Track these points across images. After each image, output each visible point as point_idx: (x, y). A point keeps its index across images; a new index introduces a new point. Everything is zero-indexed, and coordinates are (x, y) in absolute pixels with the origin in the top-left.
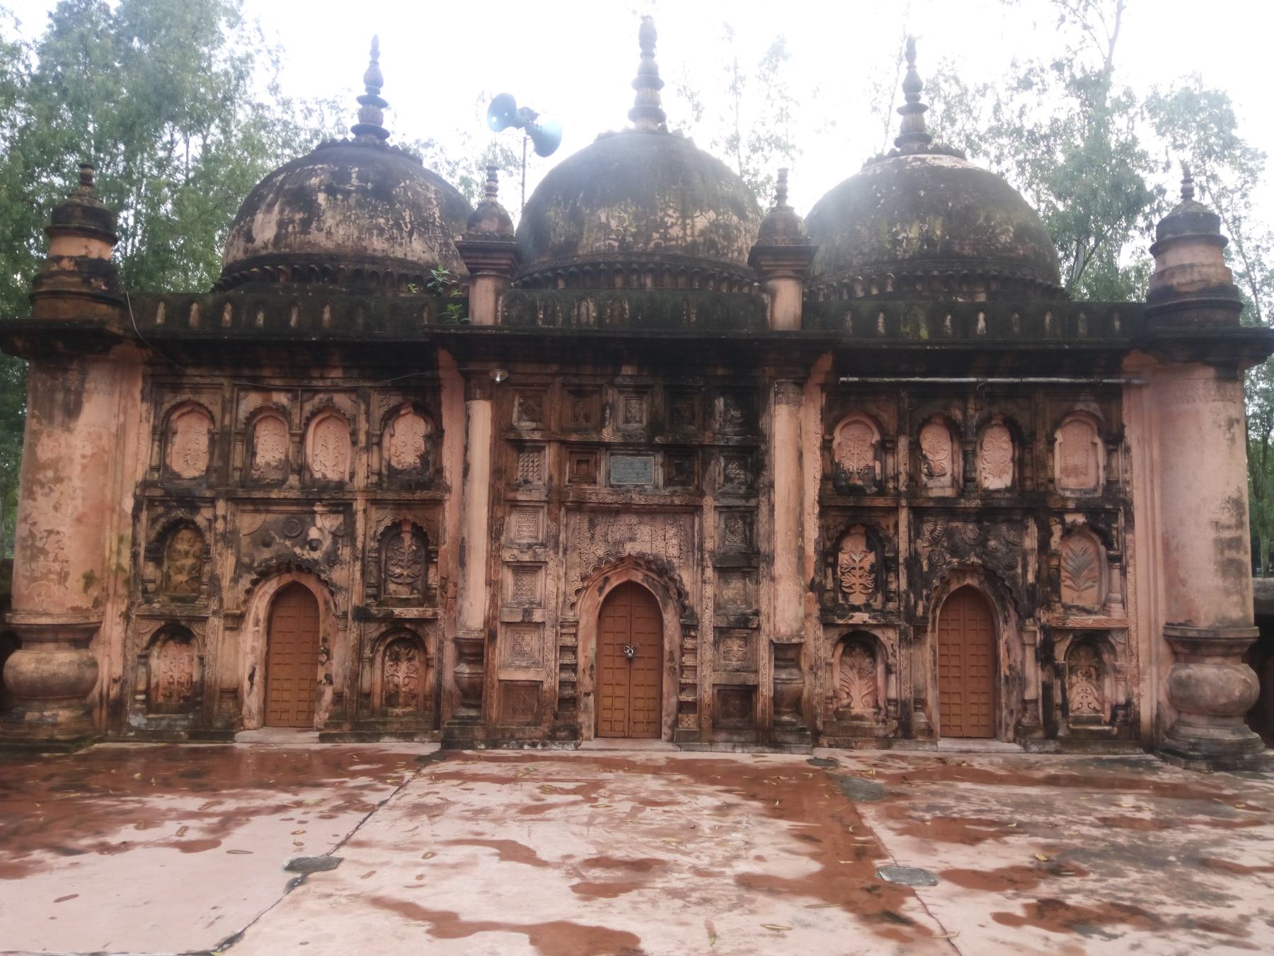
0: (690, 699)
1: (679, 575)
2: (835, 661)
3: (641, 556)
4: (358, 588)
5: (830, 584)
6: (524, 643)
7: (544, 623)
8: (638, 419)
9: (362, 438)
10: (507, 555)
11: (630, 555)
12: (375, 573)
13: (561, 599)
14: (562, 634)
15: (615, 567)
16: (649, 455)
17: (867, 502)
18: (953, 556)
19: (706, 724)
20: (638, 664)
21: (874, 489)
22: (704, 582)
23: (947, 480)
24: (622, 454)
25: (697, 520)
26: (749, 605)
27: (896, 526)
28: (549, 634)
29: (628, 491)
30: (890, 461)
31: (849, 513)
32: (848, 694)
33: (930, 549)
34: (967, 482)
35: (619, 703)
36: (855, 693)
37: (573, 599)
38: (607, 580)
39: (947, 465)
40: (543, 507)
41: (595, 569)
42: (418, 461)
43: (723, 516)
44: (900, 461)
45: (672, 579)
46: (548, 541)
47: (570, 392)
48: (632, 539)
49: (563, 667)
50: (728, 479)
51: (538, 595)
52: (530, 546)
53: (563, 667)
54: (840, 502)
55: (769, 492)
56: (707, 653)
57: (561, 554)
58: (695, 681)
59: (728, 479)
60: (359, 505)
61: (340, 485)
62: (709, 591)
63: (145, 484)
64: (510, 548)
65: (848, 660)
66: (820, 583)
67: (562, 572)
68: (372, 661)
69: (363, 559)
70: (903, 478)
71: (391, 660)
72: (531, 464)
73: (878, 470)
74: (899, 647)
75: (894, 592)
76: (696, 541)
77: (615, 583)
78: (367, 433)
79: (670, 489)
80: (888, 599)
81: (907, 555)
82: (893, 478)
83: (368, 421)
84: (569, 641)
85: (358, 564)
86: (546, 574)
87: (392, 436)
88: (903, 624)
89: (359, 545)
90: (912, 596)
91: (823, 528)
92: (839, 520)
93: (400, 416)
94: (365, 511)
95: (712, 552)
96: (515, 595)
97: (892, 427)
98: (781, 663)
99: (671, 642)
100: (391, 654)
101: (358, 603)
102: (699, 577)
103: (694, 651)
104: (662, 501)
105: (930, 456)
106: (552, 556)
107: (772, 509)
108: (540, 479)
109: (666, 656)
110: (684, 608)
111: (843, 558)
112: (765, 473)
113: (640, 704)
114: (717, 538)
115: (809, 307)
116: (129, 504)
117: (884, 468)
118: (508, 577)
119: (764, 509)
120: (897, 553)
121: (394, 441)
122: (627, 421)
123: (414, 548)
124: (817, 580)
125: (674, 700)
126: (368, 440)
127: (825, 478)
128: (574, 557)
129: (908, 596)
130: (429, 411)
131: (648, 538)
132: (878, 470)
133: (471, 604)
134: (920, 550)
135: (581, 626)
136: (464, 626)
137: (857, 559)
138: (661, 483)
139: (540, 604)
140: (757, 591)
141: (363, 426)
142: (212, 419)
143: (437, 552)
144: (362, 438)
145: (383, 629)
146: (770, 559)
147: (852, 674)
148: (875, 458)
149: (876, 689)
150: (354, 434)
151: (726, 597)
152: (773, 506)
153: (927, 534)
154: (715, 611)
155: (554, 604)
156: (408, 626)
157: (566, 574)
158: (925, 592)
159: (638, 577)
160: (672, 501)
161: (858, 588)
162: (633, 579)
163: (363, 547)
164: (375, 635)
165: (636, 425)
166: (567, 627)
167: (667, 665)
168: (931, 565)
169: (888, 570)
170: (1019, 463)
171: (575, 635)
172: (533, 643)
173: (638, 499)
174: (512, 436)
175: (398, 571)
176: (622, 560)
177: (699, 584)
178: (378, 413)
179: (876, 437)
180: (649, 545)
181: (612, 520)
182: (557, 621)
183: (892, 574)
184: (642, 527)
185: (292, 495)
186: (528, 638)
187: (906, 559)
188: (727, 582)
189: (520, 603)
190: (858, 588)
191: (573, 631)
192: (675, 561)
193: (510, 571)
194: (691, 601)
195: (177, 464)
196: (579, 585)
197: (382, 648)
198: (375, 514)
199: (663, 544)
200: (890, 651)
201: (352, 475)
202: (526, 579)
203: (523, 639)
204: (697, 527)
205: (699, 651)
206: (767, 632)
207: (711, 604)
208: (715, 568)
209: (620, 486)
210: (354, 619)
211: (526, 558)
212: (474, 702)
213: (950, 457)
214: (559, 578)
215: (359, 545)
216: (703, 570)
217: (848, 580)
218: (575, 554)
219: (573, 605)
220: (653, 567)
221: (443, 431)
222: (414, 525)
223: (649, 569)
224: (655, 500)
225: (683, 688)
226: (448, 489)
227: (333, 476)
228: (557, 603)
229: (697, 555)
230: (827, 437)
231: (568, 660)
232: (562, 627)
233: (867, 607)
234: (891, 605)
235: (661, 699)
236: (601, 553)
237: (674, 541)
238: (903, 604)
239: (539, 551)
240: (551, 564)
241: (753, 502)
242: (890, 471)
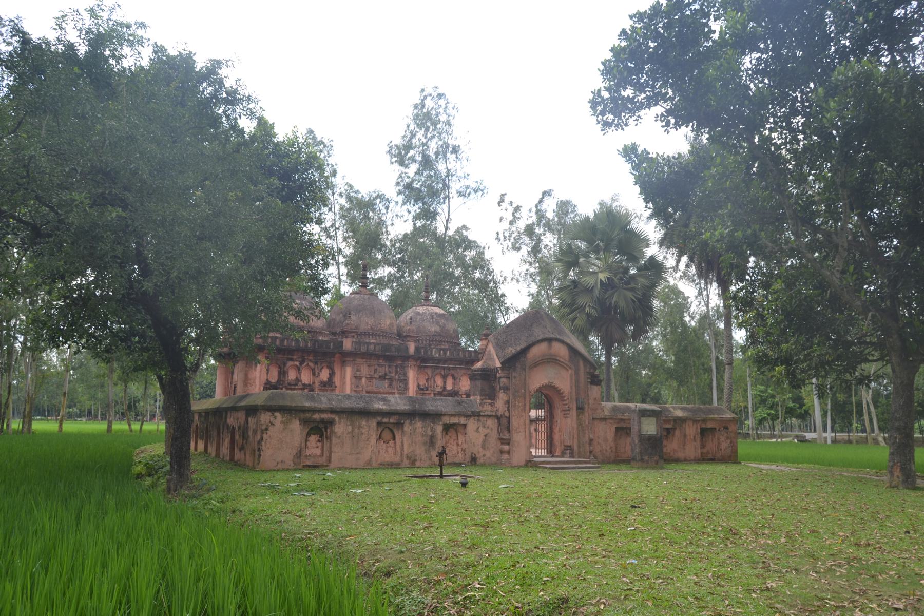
34: (444, 388)
44: (431, 383)
61: (309, 385)
63: (265, 384)
115: (417, 349)
116: (262, 388)
130: (331, 368)
142: (280, 367)
170: (454, 384)
173: (382, 390)
185: (301, 387)
195: (270, 380)
201: (314, 383)
226: (336, 387)
227: (307, 383)
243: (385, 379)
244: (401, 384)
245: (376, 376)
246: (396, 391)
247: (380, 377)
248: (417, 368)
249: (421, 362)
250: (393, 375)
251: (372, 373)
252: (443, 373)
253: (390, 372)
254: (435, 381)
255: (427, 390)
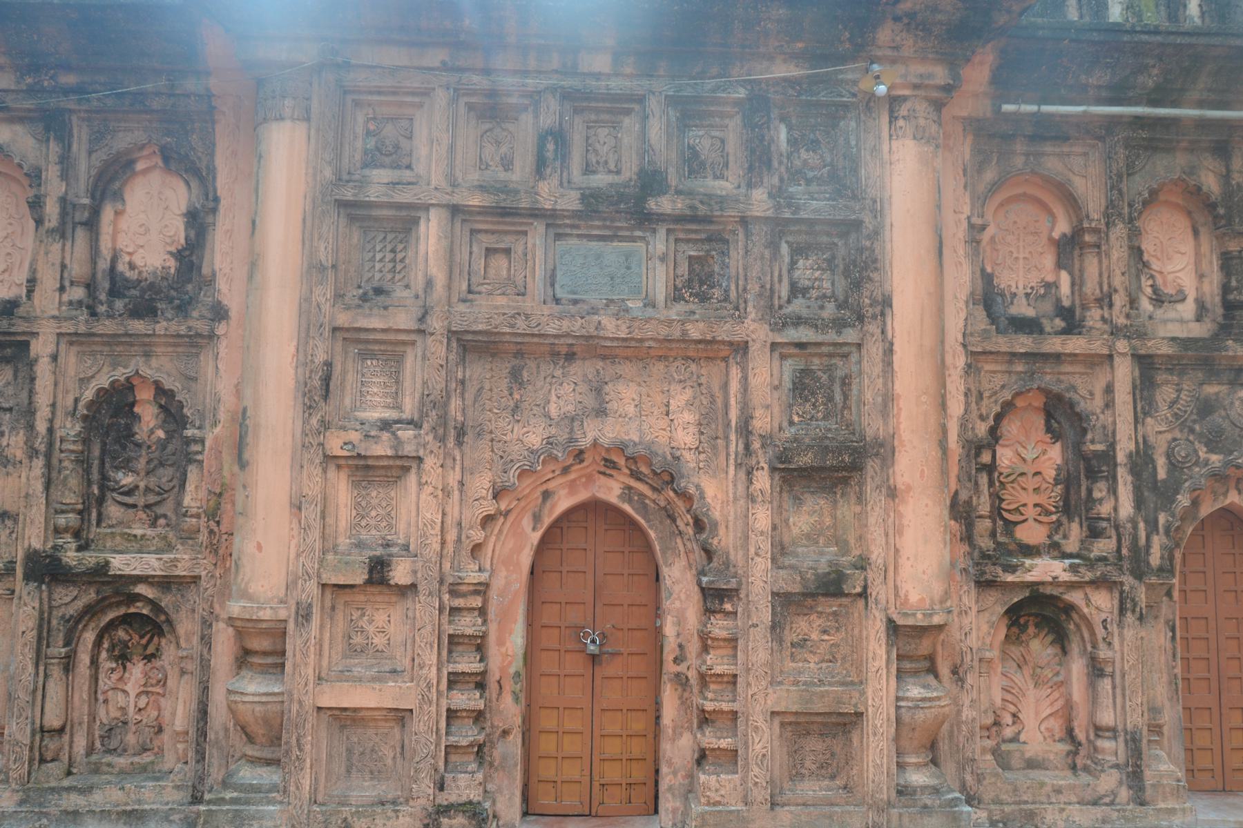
0: (724, 743)
1: (698, 487)
2: (994, 654)
3: (621, 448)
4: (37, 512)
5: (984, 505)
6: (371, 629)
7: (413, 586)
8: (612, 167)
9: (52, 210)
10: (335, 444)
11: (595, 444)
12: (74, 482)
13: (451, 536)
14: (454, 611)
15: (566, 470)
16: (633, 239)
17: (1054, 344)
18: (1211, 450)
19: (761, 794)
20: (611, 668)
21: (1059, 323)
22: (751, 498)
23: (1187, 309)
24: (579, 236)
25: (735, 373)
26: (844, 548)
27: (1109, 389)
28: (424, 609)
29: (594, 311)
30: (1092, 267)
31: (1020, 367)
32: (1014, 715)
33: (1169, 436)
35: (572, 745)
36: (1027, 716)
37: (478, 535)
38: (546, 495)
39: (1188, 282)
40: (413, 343)
41: (523, 474)
42: (172, 263)
43: (788, 363)
45: (685, 496)
46: (423, 415)
47: (470, 107)
48: (601, 412)
49: (454, 680)
50: (796, 290)
51: (402, 526)
52: (385, 425)
53: (454, 680)
54: (1002, 343)
55: (883, 314)
56: (758, 648)
57: (451, 443)
58: (735, 706)
59: (796, 290)
60: (41, 347)
62: (762, 518)
64: (344, 428)
65: (1015, 651)
66: (968, 503)
67: (453, 478)
68: (68, 664)
69: (48, 456)
70: (1119, 300)
71: (111, 657)
72: (389, 256)
73: (1065, 288)
74: (1120, 624)
75: (1108, 520)
76: (734, 415)
77: (564, 503)
78: (63, 200)
79: (680, 307)
80: (1095, 533)
81: (1132, 447)
82: (1099, 301)
83: (64, 176)
84: (467, 625)
85: (39, 463)
86: (421, 485)
87: (118, 213)
88: (1128, 580)
89: (41, 427)
90: (1142, 525)
91: (974, 396)
92: (999, 380)
93: (135, 174)
94: (54, 358)
95: (766, 440)
96: (354, 526)
97: (1094, 204)
98: (907, 665)
99: (680, 622)
100: (111, 650)
101: (37, 544)
102: (741, 488)
103: (732, 641)
104: (664, 332)
105: (1155, 265)
106: (433, 445)
107: (889, 351)
108: (407, 286)
109: (669, 657)
110: (709, 553)
111: (1005, 457)
112: (875, 276)
113: (613, 747)
114: (776, 410)
117: (1077, 284)
118: (342, 489)
119: (874, 350)
120: (1112, 446)
121: (124, 224)
122: (588, 170)
123: (161, 434)
124: (964, 496)
125: (686, 741)
126: (64, 214)
127: (972, 299)
128: (479, 451)
129: (1135, 527)
131: (631, 410)
132: (1065, 288)
133: (259, 547)
134: (1152, 439)
135: (493, 594)
136: (245, 595)
137: (1029, 456)
138: (660, 294)
139: (406, 547)
140: (861, 518)
141: (54, 187)
143: (202, 441)
144: (52, 210)
145: (91, 596)
146: (884, 450)
147: (1021, 679)
148: (1060, 265)
149: (1069, 706)
150: (36, 205)
151: (795, 531)
152: (892, 344)
153: (1164, 410)
154: (773, 560)
155: (437, 547)
156: (141, 589)
157: (461, 483)
158: (1162, 518)
159: (611, 491)
160: (684, 333)
161: (1030, 512)
162: (602, 495)
163: (51, 431)
164: (71, 611)
165: (610, 178)
166: (464, 595)
167: (670, 668)
168: (1173, 466)
169: (1092, 475)
171: (482, 611)
172: (392, 629)
173: (611, 327)
174: (348, 194)
175: (127, 480)
176: (579, 455)
177: (742, 502)
178: (84, 168)
179: (1063, 227)
180: (634, 425)
181: (558, 373)
182: (441, 582)
183: (1102, 485)
184: (621, 387)
186: (380, 618)
187: (1130, 456)
188: (798, 501)
189: (360, 545)
190: (1030, 512)
191: (477, 602)
192: (688, 456)
193: (343, 475)
194: (725, 539)
196: (489, 507)
197: (89, 637)
198: (71, 360)
199: (663, 423)
200: (1100, 632)
202: (375, 494)
203: (371, 622)
204: (734, 386)
205: (741, 643)
206: (882, 597)
207: (766, 546)
208: (773, 469)
209: (575, 302)
210: (28, 577)
211: (381, 448)
212: (267, 753)
213: (1191, 267)
214: (447, 492)
215: (41, 427)
216: (749, 473)
217: (1015, 496)
218: (484, 443)
219: (477, 549)
220: (644, 469)
221: (216, 200)
222: (160, 390)
223: (636, 475)
224: (650, 331)
225: (705, 719)
226: (220, 313)
228: (443, 543)
229: (736, 444)
230: (977, 221)
231: (467, 664)
232: (454, 593)
233: (1055, 550)
234: (1104, 546)
235: (657, 736)
236: (535, 440)
237: (689, 417)
238: (1126, 543)
239: (406, 434)
240: (430, 462)
241: (850, 335)
242: (1091, 287)
243: (646, 220)
244: (806, 271)
245: (549, 194)
246: (756, 330)
247: (592, 202)
248: (965, 149)
249: (1002, 84)
250: (723, 188)
251: (520, 173)
252: (1211, 183)
253: (693, 163)
254: (1137, 252)
255: (1072, 323)
